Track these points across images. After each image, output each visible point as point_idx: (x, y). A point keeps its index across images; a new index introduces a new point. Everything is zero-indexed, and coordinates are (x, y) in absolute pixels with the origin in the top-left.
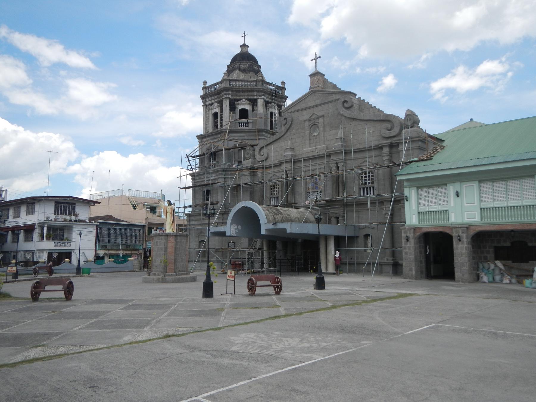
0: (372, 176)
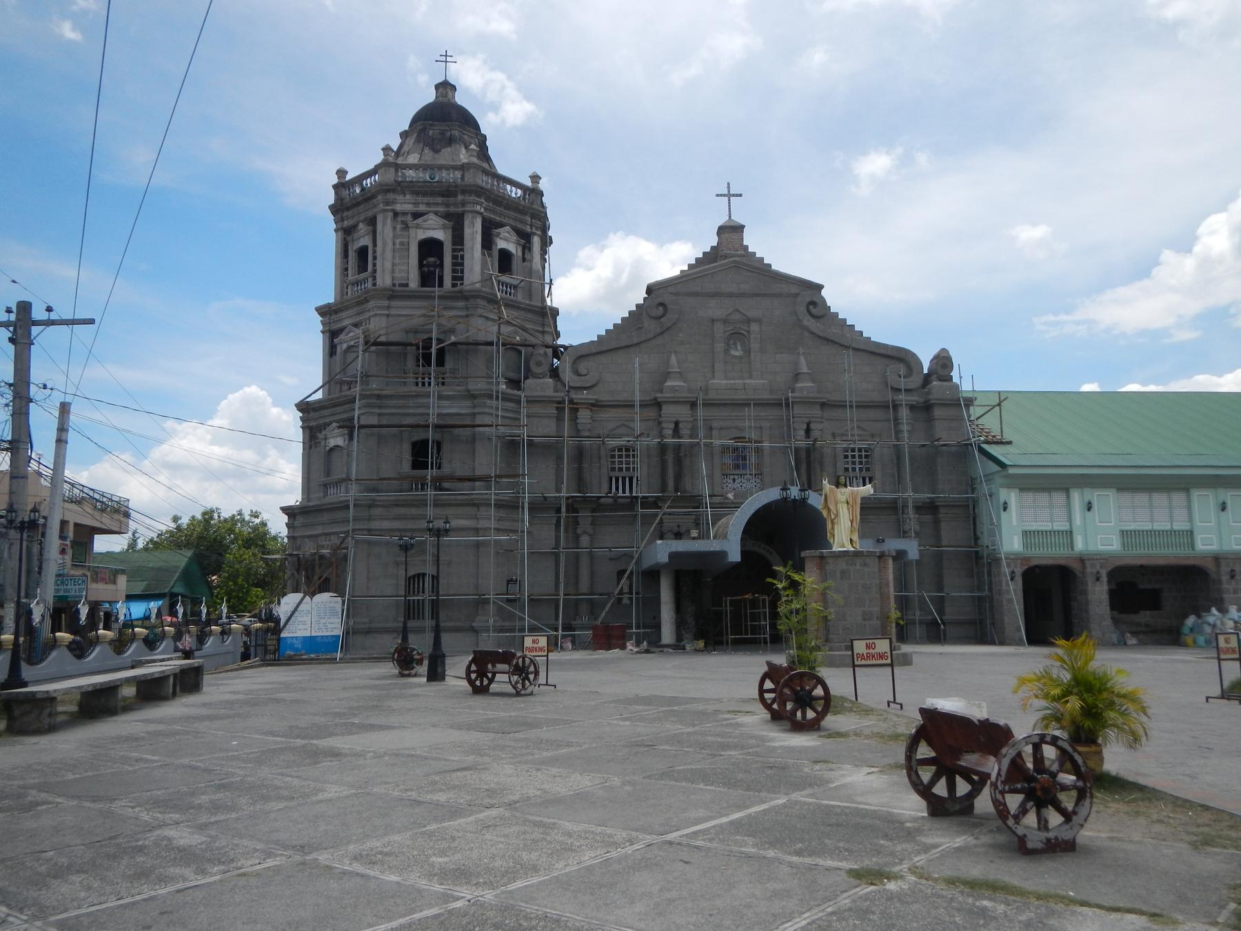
0: (866, 457)
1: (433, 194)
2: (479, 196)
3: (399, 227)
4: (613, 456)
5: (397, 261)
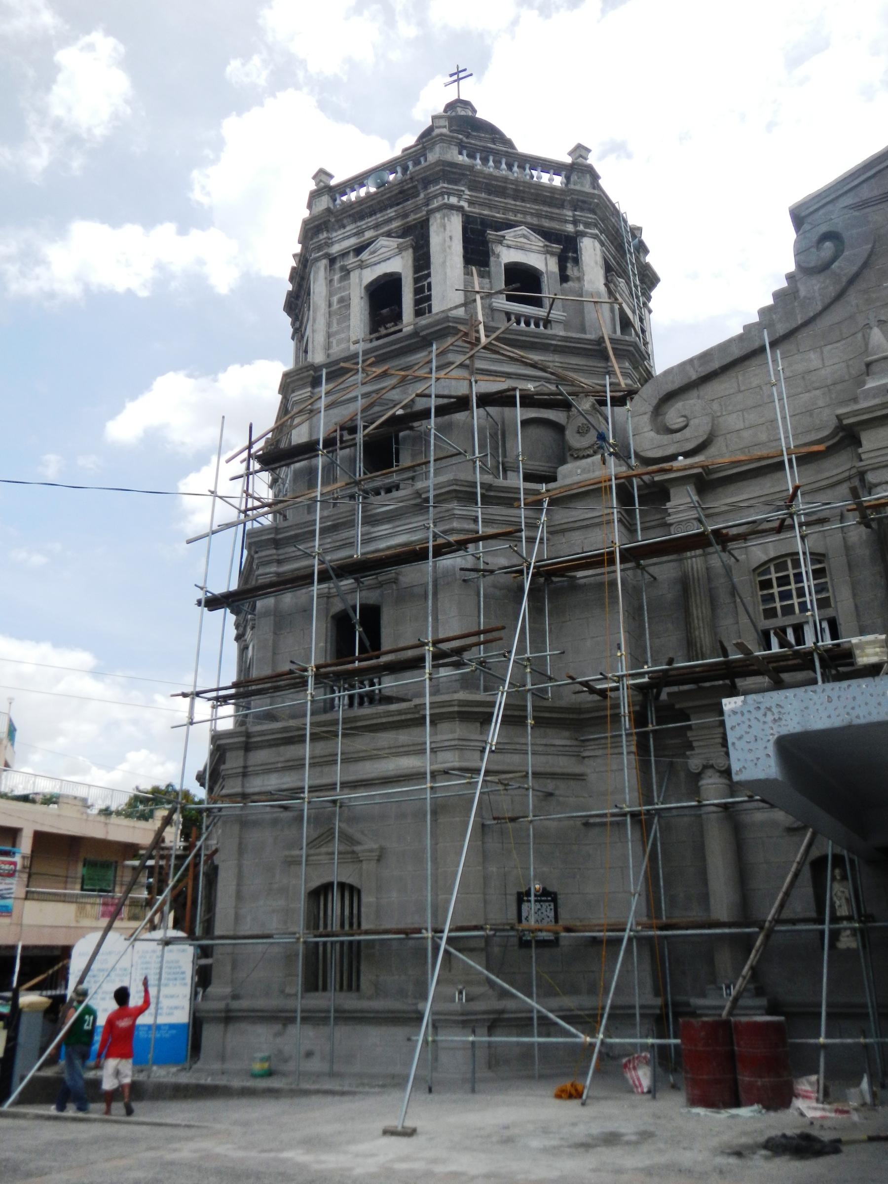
1: (383, 209)
2: (455, 182)
3: (336, 277)
4: (766, 585)
5: (335, 327)
